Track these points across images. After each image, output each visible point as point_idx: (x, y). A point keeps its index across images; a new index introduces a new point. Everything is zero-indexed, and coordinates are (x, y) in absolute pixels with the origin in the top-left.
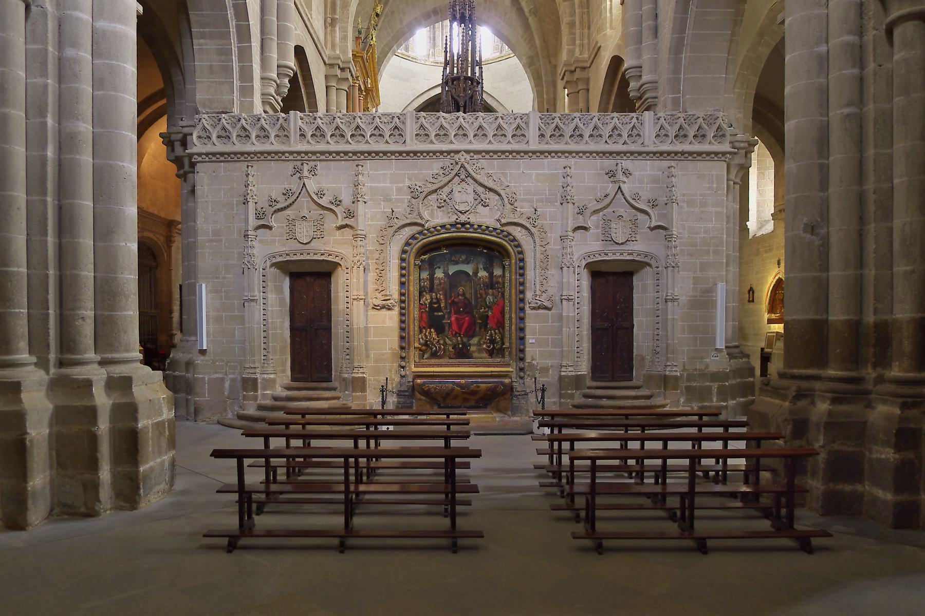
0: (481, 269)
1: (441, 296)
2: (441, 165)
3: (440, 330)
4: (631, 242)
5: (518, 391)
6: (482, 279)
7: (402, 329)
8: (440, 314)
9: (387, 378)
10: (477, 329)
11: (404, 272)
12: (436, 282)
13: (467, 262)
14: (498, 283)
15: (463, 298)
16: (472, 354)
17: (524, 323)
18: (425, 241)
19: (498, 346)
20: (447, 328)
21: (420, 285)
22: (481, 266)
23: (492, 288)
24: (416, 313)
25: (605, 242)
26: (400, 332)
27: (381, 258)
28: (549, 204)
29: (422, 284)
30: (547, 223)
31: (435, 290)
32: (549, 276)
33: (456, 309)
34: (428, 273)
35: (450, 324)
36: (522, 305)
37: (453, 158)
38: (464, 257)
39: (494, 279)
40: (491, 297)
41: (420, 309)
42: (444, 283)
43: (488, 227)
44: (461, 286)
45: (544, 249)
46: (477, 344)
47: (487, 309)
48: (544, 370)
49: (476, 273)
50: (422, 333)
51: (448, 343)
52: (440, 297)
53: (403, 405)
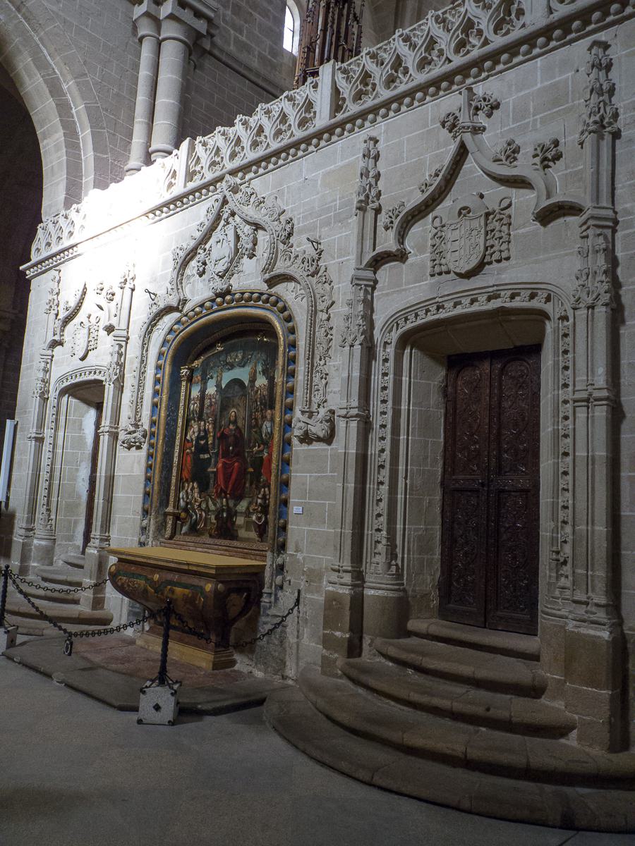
1: (210, 426)
3: (203, 488)
4: (495, 265)
5: (268, 615)
7: (148, 479)
12: (207, 402)
13: (242, 365)
16: (237, 531)
22: (260, 368)
25: (437, 278)
28: (340, 224)
33: (224, 448)
35: (215, 474)
42: (215, 403)
44: (233, 406)
48: (314, 577)
49: (253, 380)
52: (208, 429)
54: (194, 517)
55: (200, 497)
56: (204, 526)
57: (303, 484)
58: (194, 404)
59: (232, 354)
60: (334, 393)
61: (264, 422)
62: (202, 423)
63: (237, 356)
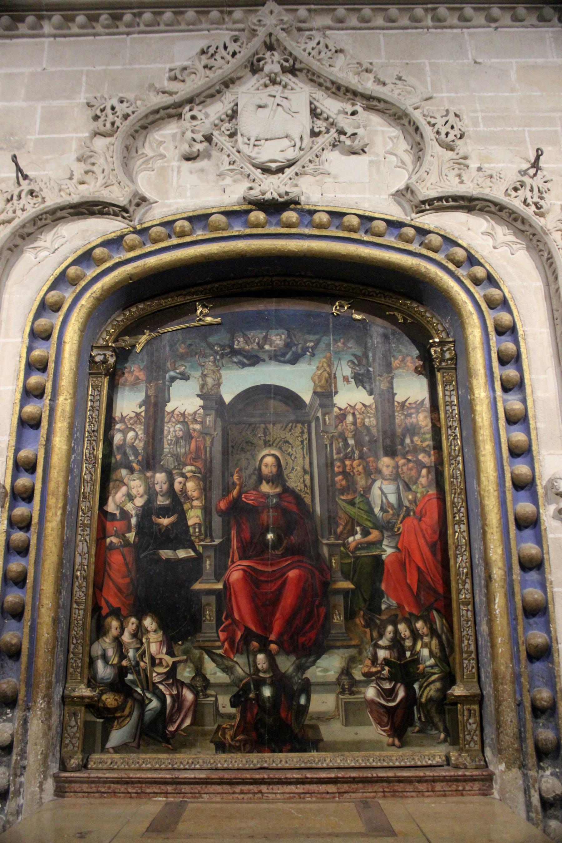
0: (346, 379)
1: (190, 485)
2: (203, 44)
6: (350, 418)
8: (182, 554)
10: (338, 619)
11: (35, 379)
14: (413, 430)
15: (278, 490)
16: (315, 728)
17: (543, 585)
18: (128, 269)
19: (432, 691)
20: (209, 615)
21: (108, 441)
23: (391, 452)
24: (82, 547)
29: (118, 438)
31: (168, 461)
33: (248, 535)
34: (141, 396)
37: (241, 26)
39: (399, 418)
40: (389, 488)
41: (102, 534)
42: (204, 433)
43: (366, 219)
44: (267, 444)
46: (338, 682)
47: (374, 535)
51: (212, 680)
52: (184, 491)
54: (154, 704)
55: (170, 653)
56: (193, 723)
58: (124, 433)
59: (251, 334)
61: (374, 481)
62: (160, 477)
63: (266, 339)
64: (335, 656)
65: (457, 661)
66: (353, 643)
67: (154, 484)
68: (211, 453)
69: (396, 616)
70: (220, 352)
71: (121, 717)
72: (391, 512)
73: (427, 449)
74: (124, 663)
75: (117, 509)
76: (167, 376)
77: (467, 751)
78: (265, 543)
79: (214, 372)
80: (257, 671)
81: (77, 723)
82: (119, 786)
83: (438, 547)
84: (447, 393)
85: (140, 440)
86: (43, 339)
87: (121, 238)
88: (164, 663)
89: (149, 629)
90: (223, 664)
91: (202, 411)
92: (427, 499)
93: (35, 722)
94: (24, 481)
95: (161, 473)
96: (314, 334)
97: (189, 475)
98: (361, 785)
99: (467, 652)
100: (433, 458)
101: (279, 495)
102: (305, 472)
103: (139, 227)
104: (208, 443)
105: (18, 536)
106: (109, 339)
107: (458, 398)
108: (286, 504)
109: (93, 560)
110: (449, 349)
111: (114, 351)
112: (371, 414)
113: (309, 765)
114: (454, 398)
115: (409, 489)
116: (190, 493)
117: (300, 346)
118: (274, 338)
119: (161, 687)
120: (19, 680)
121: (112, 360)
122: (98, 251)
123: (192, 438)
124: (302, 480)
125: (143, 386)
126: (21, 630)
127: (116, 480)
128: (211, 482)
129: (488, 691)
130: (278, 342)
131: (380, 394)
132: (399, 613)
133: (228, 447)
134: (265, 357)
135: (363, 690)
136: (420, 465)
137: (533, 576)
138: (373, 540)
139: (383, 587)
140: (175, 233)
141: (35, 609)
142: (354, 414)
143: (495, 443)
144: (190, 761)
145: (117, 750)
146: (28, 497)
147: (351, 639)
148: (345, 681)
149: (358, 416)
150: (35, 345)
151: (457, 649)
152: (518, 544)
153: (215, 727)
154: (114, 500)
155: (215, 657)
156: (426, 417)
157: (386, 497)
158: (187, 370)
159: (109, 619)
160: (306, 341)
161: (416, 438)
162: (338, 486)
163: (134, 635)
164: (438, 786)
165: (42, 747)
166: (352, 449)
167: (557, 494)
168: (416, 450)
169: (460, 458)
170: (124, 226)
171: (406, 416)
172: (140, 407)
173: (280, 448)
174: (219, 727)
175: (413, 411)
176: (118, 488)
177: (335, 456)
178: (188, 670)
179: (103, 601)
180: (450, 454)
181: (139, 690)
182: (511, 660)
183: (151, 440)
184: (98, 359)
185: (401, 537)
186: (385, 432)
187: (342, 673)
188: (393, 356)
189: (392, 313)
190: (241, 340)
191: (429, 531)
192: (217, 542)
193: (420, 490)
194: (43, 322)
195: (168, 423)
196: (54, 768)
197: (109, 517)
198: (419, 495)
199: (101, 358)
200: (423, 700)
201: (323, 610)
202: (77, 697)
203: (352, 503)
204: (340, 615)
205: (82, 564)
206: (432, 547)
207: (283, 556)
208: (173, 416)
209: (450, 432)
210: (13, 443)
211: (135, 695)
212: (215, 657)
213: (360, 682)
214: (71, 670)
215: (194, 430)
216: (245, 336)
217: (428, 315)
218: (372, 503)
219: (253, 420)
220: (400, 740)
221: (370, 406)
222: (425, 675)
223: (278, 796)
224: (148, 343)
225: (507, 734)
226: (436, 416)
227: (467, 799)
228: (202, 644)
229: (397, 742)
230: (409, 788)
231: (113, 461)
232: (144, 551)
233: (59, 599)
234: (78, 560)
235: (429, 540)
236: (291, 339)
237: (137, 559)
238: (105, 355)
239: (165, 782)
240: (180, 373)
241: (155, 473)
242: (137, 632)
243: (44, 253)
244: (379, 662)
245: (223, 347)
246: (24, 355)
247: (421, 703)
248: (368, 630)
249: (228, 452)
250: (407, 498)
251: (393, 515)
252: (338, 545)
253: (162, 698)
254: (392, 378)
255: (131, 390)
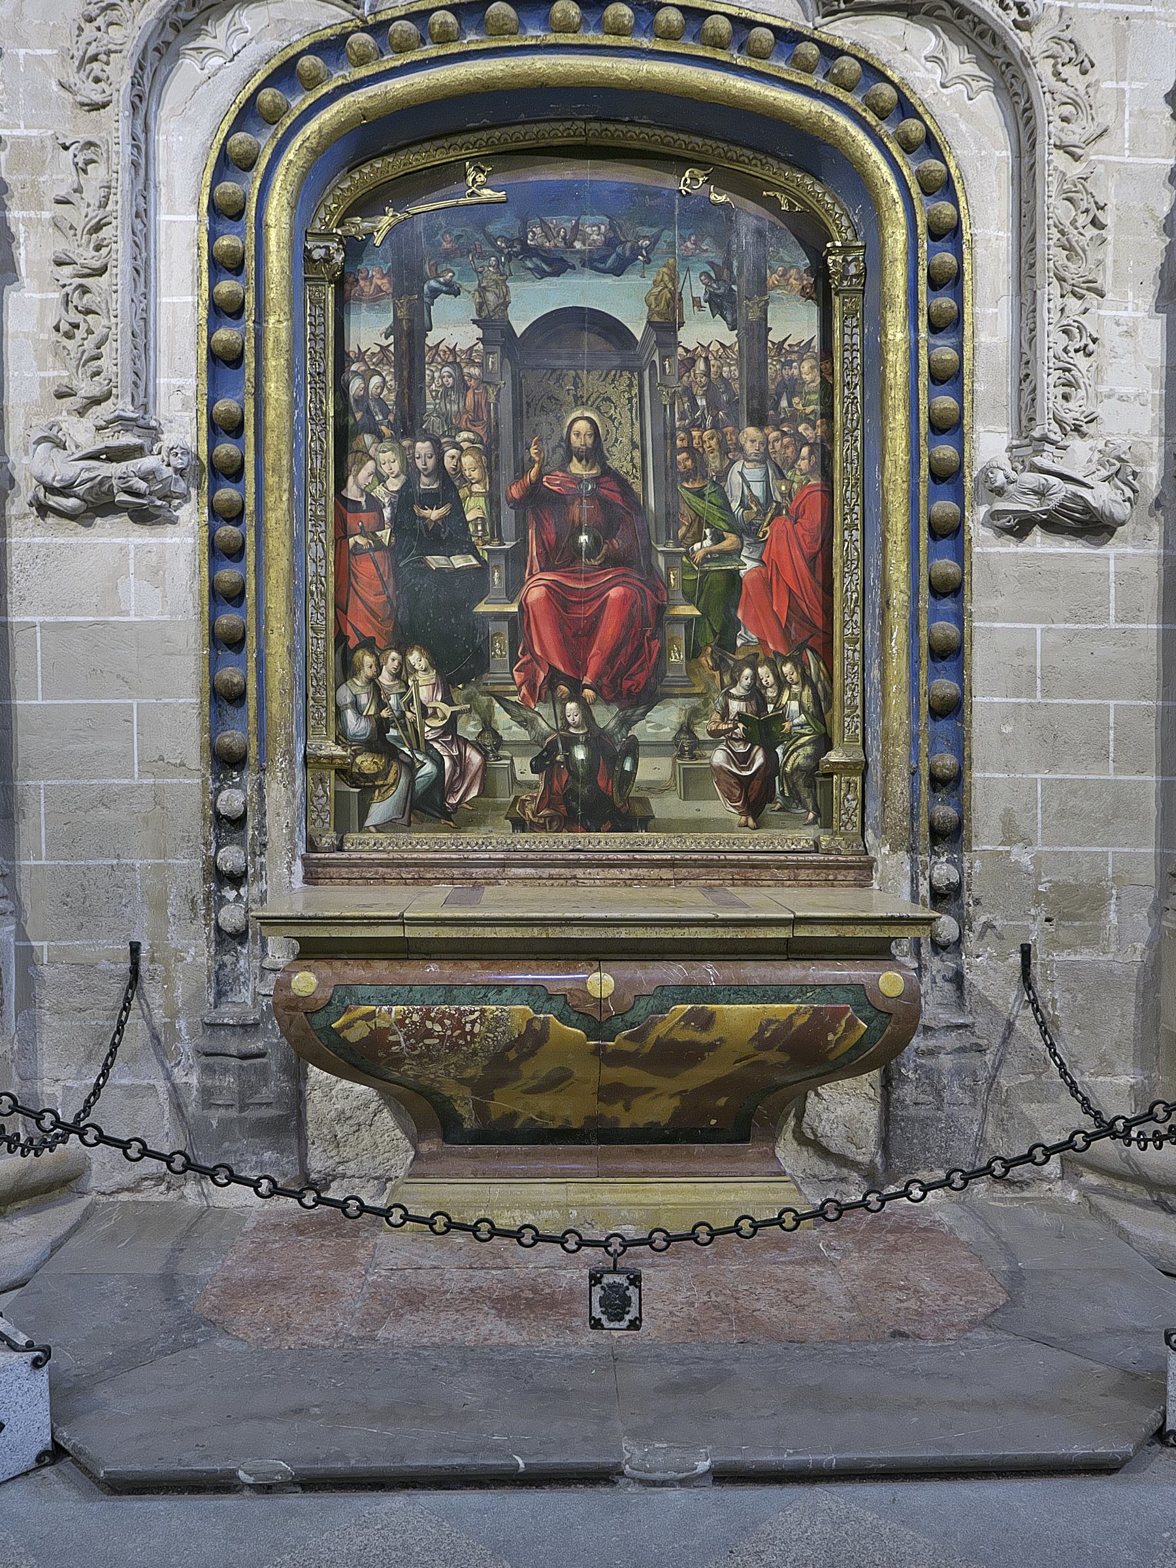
0: (696, 302)
6: (701, 365)
8: (459, 562)
9: (135, 948)
10: (677, 657)
12: (437, 376)
14: (792, 387)
16: (644, 802)
19: (800, 758)
20: (500, 649)
21: (341, 390)
22: (695, 287)
23: (759, 420)
26: (214, 664)
27: (92, 195)
29: (355, 386)
30: (1097, 13)
31: (433, 423)
32: (1110, 336)
34: (388, 320)
35: (518, 624)
36: (945, 508)
38: (595, 231)
39: (773, 367)
40: (754, 473)
44: (579, 401)
45: (1077, 169)
47: (730, 541)
50: (355, 674)
51: (505, 738)
52: (458, 469)
53: (233, 1113)
55: (448, 700)
57: (1020, 653)
58: (366, 377)
59: (552, 221)
60: (1121, 399)
61: (733, 462)
62: (423, 447)
64: (672, 707)
65: (836, 719)
66: (697, 690)
67: (414, 458)
68: (496, 413)
69: (756, 655)
70: (506, 251)
71: (383, 785)
72: (755, 509)
73: (812, 417)
74: (384, 714)
75: (362, 496)
76: (426, 287)
77: (842, 835)
78: (577, 549)
79: (497, 284)
80: (569, 725)
81: (325, 792)
82: (389, 870)
83: (819, 561)
84: (848, 331)
85: (389, 389)
86: (231, 218)
87: (343, 37)
88: (440, 714)
89: (417, 667)
90: (521, 715)
91: (480, 345)
92: (807, 491)
93: (274, 786)
94: (226, 448)
95: (424, 441)
96: (651, 226)
97: (465, 445)
98: (703, 870)
99: (849, 707)
100: (819, 431)
101: (595, 479)
102: (634, 446)
103: (371, 20)
104: (492, 399)
105: (227, 531)
106: (330, 220)
107: (862, 340)
108: (605, 492)
109: (331, 569)
110: (856, 259)
111: (340, 242)
112: (732, 359)
113: (636, 847)
114: (857, 339)
115: (783, 477)
116: (467, 473)
117: (629, 244)
118: (588, 230)
119: (436, 745)
120: (246, 732)
121: (339, 258)
122: (307, 62)
123: (468, 388)
124: (629, 458)
125: (388, 302)
126: (243, 664)
127: (357, 452)
128: (497, 456)
129: (875, 756)
130: (596, 237)
131: (746, 329)
132: (760, 652)
133: (521, 405)
134: (574, 260)
135: (708, 753)
136: (803, 441)
137: (948, 604)
138: (729, 548)
139: (740, 616)
140: (431, 36)
141: (262, 637)
142: (706, 359)
143: (911, 412)
144: (480, 842)
145: (379, 828)
146: (235, 474)
147: (694, 685)
148: (685, 741)
149: (712, 362)
150: (219, 228)
151: (837, 703)
152: (930, 559)
153: (511, 799)
154: (356, 482)
155: (509, 707)
156: (812, 368)
157: (749, 487)
158: (455, 279)
159: (359, 653)
160: (638, 238)
161: (796, 400)
162: (681, 468)
163: (397, 676)
164: (803, 874)
165: (286, 818)
166: (703, 412)
167: (991, 491)
168: (795, 418)
169: (858, 433)
170: (347, 15)
171: (783, 365)
172: (387, 338)
173: (598, 408)
174: (516, 798)
175: (794, 357)
176: (362, 464)
177: (677, 424)
178: (472, 723)
179: (349, 627)
180: (844, 425)
181: (406, 750)
182: (908, 714)
183: (406, 390)
184: (317, 254)
185: (768, 546)
186: (751, 390)
187: (681, 731)
188: (770, 267)
189: (771, 194)
190: (538, 230)
191: (808, 540)
192: (508, 545)
193: (796, 479)
194: (228, 186)
195: (430, 364)
196: (301, 850)
197: (349, 506)
198: (795, 486)
199: (322, 252)
200: (788, 769)
201: (656, 645)
202: (325, 757)
203: (699, 493)
204: (679, 652)
205: (316, 574)
206: (811, 561)
207: (601, 567)
208: (437, 353)
209: (846, 392)
210: (204, 389)
211: (401, 756)
212: (509, 707)
213: (705, 742)
214: (312, 722)
215: (470, 376)
216: (543, 224)
217: (827, 198)
218: (729, 494)
219: (559, 363)
220: (754, 820)
221: (729, 348)
222: (791, 737)
223: (597, 882)
224: (393, 229)
225: (895, 809)
226: (828, 366)
227: (837, 890)
228: (490, 688)
229: (751, 822)
230: (766, 874)
231: (351, 421)
232: (404, 558)
233: (294, 622)
234: (311, 568)
235: (807, 551)
236: (615, 232)
237: (395, 570)
238: (327, 248)
239: (451, 865)
240: (446, 284)
241: (416, 441)
242: (401, 671)
243: (216, 61)
244: (731, 717)
245: (510, 242)
246: (205, 245)
247: (785, 773)
248: (717, 673)
249: (522, 412)
250: (779, 489)
251: (758, 513)
252: (680, 554)
253: (439, 762)
254: (767, 303)
255: (370, 309)
